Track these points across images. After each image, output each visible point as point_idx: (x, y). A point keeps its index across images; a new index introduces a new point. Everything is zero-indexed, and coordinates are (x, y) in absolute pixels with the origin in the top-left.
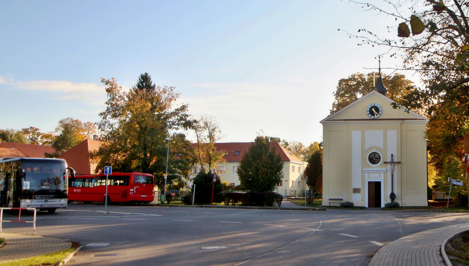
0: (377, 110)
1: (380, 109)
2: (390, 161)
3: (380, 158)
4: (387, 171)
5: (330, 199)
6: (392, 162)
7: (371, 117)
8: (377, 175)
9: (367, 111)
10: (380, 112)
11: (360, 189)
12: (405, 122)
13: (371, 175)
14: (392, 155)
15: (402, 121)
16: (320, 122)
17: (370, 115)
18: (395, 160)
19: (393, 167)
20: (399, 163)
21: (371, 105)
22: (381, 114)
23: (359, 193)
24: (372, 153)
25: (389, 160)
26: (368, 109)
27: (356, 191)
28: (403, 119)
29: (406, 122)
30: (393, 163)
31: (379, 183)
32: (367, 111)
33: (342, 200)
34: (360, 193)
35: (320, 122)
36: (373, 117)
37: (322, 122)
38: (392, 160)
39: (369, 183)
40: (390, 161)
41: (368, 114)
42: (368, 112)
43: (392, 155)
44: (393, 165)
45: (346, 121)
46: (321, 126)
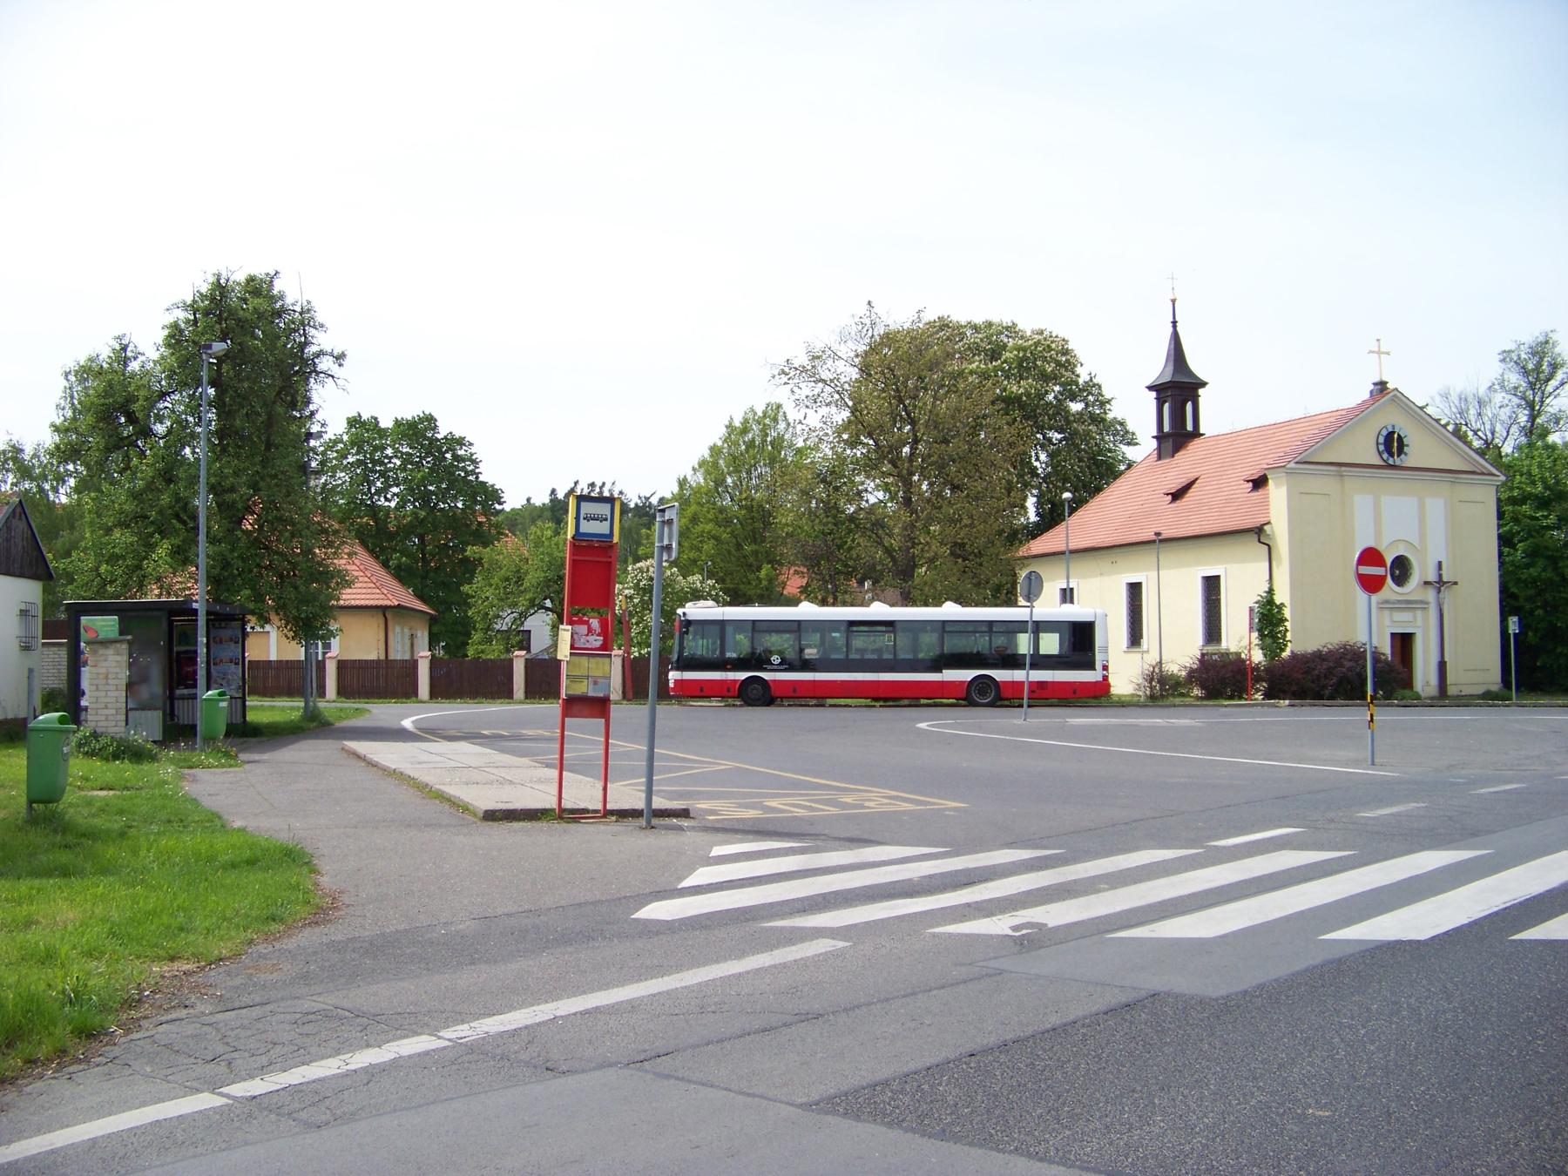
12: (1461, 478)
13: (1399, 616)
14: (1440, 563)
25: (1432, 577)
29: (1461, 478)
39: (1392, 634)
43: (1440, 563)
45: (1343, 469)
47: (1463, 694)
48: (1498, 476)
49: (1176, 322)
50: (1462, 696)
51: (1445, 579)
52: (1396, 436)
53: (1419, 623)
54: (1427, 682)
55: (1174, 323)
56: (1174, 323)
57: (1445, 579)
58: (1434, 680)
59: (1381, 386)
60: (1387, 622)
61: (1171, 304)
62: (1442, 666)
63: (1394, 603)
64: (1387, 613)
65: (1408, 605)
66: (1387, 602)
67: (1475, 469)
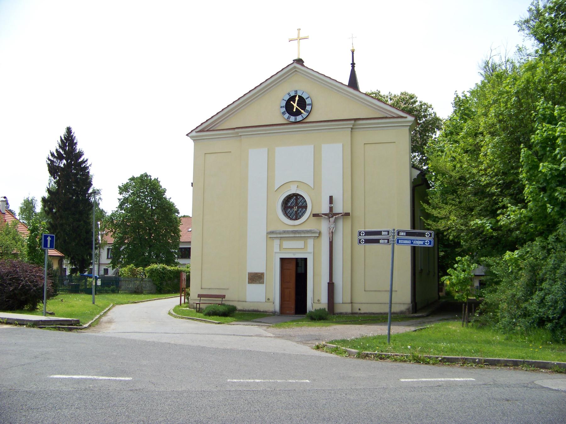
0: (302, 103)
1: (308, 101)
2: (327, 211)
3: (306, 207)
4: (320, 233)
5: (200, 296)
6: (331, 214)
7: (289, 118)
8: (299, 244)
9: (281, 107)
10: (308, 108)
11: (262, 274)
13: (287, 244)
14: (331, 198)
15: (353, 122)
16: (187, 135)
17: (287, 115)
18: (339, 208)
19: (332, 226)
20: (347, 214)
21: (289, 94)
22: (309, 113)
23: (260, 283)
24: (289, 198)
26: (284, 103)
27: (256, 278)
28: (356, 120)
30: (332, 217)
31: (305, 260)
32: (281, 107)
33: (224, 296)
34: (263, 283)
35: (186, 135)
36: (292, 119)
37: (194, 134)
38: (331, 209)
39: (282, 260)
40: (327, 211)
41: (284, 113)
42: (284, 109)
43: (331, 198)
44: (332, 220)
45: (236, 130)
46: (190, 143)
47: (362, 311)
48: (406, 117)
49: (355, 64)
50: (361, 314)
51: (335, 211)
52: (297, 98)
53: (310, 248)
54: (319, 300)
55: (353, 65)
56: (353, 65)
57: (335, 211)
58: (324, 299)
59: (300, 61)
60: (277, 249)
61: (351, 53)
62: (331, 286)
63: (280, 233)
64: (277, 242)
65: (296, 235)
66: (272, 233)
67: (385, 115)
